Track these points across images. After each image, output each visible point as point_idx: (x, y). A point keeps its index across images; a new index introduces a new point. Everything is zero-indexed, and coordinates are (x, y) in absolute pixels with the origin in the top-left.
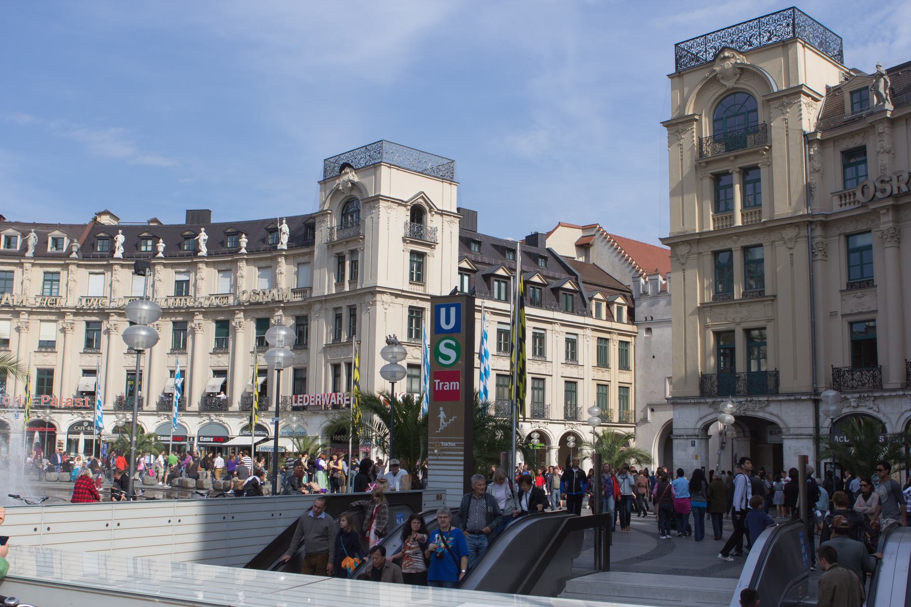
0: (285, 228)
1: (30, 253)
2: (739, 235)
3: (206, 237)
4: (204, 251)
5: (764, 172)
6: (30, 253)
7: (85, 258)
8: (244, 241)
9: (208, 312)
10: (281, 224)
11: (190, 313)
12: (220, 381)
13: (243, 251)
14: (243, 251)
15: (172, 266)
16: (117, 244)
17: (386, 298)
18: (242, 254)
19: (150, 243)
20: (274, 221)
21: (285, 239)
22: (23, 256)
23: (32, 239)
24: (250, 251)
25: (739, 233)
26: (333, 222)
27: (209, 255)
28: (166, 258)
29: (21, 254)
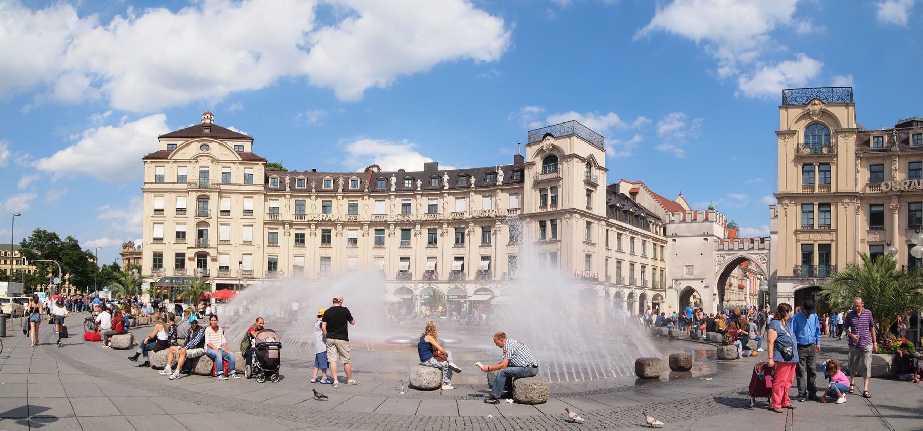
0: (501, 172)
1: (340, 190)
2: (818, 197)
4: (447, 186)
5: (833, 168)
6: (340, 190)
7: (373, 191)
8: (473, 180)
9: (449, 223)
11: (440, 223)
12: (460, 263)
15: (427, 195)
17: (577, 215)
21: (501, 179)
23: (341, 182)
24: (477, 187)
25: (818, 196)
27: (450, 189)
28: (422, 190)
29: (335, 191)
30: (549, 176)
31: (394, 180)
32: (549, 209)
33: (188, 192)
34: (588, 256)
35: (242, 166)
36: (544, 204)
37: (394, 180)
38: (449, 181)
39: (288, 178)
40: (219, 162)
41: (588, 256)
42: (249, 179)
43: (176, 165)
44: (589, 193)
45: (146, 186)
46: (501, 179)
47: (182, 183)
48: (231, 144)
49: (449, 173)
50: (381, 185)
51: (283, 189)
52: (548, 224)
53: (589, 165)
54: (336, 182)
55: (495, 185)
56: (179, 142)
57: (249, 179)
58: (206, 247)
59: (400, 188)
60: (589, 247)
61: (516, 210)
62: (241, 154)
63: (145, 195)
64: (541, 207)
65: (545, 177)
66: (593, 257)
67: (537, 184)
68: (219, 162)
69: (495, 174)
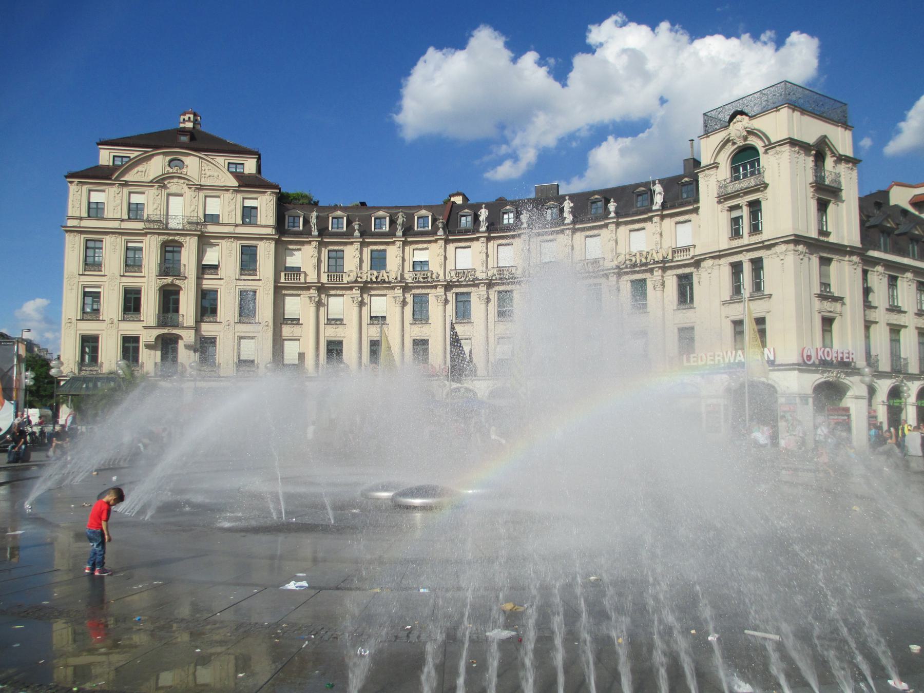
0: (658, 188)
3: (572, 205)
8: (612, 206)
10: (654, 184)
13: (612, 215)
14: (612, 215)
16: (481, 219)
18: (612, 218)
19: (511, 215)
20: (646, 185)
21: (658, 199)
22: (394, 235)
26: (724, 172)
27: (574, 222)
30: (744, 184)
31: (484, 213)
32: (746, 239)
33: (145, 234)
34: (828, 322)
35: (239, 196)
36: (736, 234)
37: (484, 213)
38: (573, 212)
39: (314, 214)
40: (201, 188)
41: (828, 322)
42: (249, 214)
43: (126, 190)
44: (823, 207)
45: (70, 223)
46: (658, 199)
47: (137, 220)
48: (222, 160)
49: (572, 197)
50: (466, 222)
51: (307, 232)
52: (747, 268)
53: (820, 158)
54: (393, 222)
55: (651, 211)
56: (134, 153)
57: (249, 214)
58: (176, 325)
59: (494, 225)
60: (827, 305)
61: (686, 249)
62: (239, 176)
63: (69, 238)
64: (732, 238)
65: (738, 186)
66: (835, 326)
67: (723, 198)
68: (201, 188)
69: (652, 193)
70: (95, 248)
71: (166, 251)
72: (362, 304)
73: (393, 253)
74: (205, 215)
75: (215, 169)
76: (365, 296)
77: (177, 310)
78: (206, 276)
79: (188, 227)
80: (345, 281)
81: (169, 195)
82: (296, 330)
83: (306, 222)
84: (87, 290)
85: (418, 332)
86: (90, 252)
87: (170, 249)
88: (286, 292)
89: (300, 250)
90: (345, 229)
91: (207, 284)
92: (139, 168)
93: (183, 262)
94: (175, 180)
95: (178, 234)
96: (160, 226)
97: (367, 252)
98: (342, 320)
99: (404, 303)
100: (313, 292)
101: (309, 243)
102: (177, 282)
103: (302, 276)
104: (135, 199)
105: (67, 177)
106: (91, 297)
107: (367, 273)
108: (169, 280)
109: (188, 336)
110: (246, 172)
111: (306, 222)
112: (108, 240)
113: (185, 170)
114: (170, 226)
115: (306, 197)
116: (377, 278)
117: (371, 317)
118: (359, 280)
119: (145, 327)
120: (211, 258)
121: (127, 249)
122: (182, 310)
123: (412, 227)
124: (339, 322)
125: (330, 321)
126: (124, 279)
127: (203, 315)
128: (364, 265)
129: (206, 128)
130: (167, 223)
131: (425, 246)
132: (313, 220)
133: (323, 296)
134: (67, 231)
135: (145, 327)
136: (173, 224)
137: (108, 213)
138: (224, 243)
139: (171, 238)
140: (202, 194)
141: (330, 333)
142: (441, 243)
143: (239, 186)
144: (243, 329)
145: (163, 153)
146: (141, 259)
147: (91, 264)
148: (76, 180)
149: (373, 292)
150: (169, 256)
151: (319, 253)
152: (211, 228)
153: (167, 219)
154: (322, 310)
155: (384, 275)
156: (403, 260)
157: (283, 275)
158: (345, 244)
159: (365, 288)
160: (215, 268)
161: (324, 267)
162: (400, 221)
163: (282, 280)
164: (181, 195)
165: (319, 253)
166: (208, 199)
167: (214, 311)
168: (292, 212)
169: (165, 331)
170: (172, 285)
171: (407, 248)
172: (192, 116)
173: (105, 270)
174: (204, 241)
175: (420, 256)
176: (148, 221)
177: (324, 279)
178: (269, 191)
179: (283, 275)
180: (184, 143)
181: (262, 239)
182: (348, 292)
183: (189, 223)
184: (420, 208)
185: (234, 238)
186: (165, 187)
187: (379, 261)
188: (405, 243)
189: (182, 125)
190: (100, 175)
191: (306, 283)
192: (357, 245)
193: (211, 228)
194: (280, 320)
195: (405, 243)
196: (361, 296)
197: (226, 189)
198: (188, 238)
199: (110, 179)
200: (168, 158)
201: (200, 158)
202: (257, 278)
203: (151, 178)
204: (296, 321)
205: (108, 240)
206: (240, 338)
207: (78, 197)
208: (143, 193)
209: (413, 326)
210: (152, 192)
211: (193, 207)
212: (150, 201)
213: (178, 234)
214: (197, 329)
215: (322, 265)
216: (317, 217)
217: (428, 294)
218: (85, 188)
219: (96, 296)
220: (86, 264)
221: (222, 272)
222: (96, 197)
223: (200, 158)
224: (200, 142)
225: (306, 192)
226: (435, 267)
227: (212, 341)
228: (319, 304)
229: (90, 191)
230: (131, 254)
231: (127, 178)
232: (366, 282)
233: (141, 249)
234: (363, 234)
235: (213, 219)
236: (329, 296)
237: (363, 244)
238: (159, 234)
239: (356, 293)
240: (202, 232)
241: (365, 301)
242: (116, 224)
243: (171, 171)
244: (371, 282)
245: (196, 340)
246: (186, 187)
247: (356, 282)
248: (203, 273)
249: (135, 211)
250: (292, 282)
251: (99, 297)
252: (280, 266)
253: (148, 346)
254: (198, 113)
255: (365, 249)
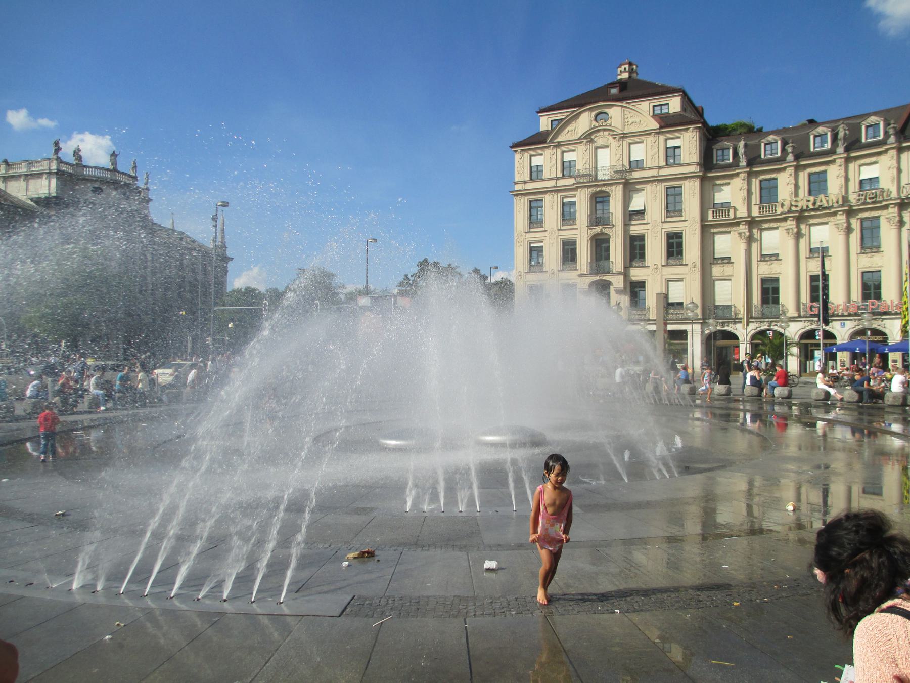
33: (577, 188)
35: (662, 138)
40: (624, 136)
42: (671, 154)
43: (559, 151)
45: (518, 187)
47: (570, 176)
48: (645, 106)
56: (561, 115)
57: (671, 154)
58: (608, 272)
68: (624, 136)
70: (537, 208)
71: (596, 203)
72: (798, 235)
73: (834, 174)
74: (630, 162)
75: (641, 114)
76: (803, 226)
77: (608, 258)
78: (633, 222)
79: (615, 176)
80: (778, 212)
81: (596, 148)
82: (727, 269)
83: (736, 154)
84: (533, 245)
85: (867, 262)
86: (534, 212)
87: (599, 199)
88: (715, 230)
89: (728, 184)
90: (731, 160)
91: (635, 230)
92: (569, 128)
93: (611, 210)
94: (601, 133)
95: (604, 185)
96: (591, 179)
97: (803, 177)
98: (777, 255)
99: (849, 230)
100: (743, 228)
101: (737, 175)
102: (606, 231)
103: (732, 211)
104: (568, 157)
105: (511, 147)
106: (535, 252)
107: (804, 200)
108: (598, 229)
109: (617, 282)
110: (671, 111)
111: (736, 154)
112: (547, 199)
113: (609, 122)
114: (600, 177)
115: (743, 125)
116: (814, 204)
117: (811, 250)
118: (793, 209)
119: (581, 276)
120: (637, 203)
121: (563, 204)
122: (612, 258)
123: (859, 140)
124: (774, 257)
125: (764, 258)
126: (562, 233)
127: (632, 260)
128: (801, 192)
129: (644, 75)
130: (596, 175)
131: (873, 159)
132: (741, 150)
133: (755, 231)
134: (515, 195)
135: (581, 276)
136: (600, 176)
137: (546, 174)
138: (648, 187)
139: (598, 189)
140: (625, 143)
141: (763, 270)
142: (893, 153)
143: (661, 127)
144: (673, 271)
145: (589, 109)
146: (575, 211)
147: (534, 221)
148: (519, 149)
149: (812, 221)
150: (599, 206)
151: (749, 184)
152: (636, 175)
153: (596, 171)
154: (755, 246)
155: (822, 200)
156: (847, 179)
157: (710, 212)
158: (779, 170)
159: (801, 217)
160: (641, 213)
161: (755, 198)
162: (841, 135)
163: (710, 218)
164: (607, 147)
165: (749, 184)
166: (632, 146)
167: (642, 256)
168: (720, 145)
169: (597, 278)
170: (602, 233)
171: (851, 166)
172: (627, 67)
173: (546, 226)
174: (630, 188)
175: (868, 172)
176: (579, 176)
177: (755, 212)
178: (691, 127)
179: (710, 212)
180: (614, 95)
181: (685, 178)
182: (783, 224)
183: (615, 172)
184: (868, 115)
185: (658, 180)
186: (592, 141)
187: (818, 184)
188: (848, 160)
189: (619, 78)
190: (538, 140)
191: (735, 218)
192: (791, 170)
193: (636, 175)
194: (708, 259)
195: (848, 160)
196: (798, 227)
197: (647, 133)
198: (614, 187)
199: (545, 142)
200: (594, 113)
201: (622, 107)
202: (683, 218)
203: (580, 135)
204: (727, 260)
205: (547, 199)
206: (668, 281)
207: (521, 162)
208: (642, 142)
209: (861, 256)
210: (581, 148)
211: (618, 156)
212: (578, 157)
213: (604, 185)
214: (626, 274)
215: (753, 197)
216: (746, 146)
217: (879, 217)
218: (527, 155)
219: (540, 250)
220: (668, 211)
221: (648, 217)
222: (536, 161)
223: (622, 107)
224: (630, 90)
225: (746, 120)
226: (887, 183)
227: (641, 285)
228: (750, 240)
229: (531, 156)
230: (567, 209)
231: (559, 139)
232: (802, 211)
233: (574, 203)
234: (797, 158)
235: (637, 165)
236: (762, 230)
237: (798, 168)
238: (588, 187)
239: (791, 224)
240: (627, 180)
241: (803, 232)
242: (551, 183)
243: (597, 124)
244: (808, 210)
245: (625, 284)
246: (610, 138)
247: (790, 211)
248: (630, 220)
249: (567, 168)
250: (720, 219)
251: (542, 251)
252: (706, 203)
253: (618, 292)
254: (633, 61)
255: (801, 174)
